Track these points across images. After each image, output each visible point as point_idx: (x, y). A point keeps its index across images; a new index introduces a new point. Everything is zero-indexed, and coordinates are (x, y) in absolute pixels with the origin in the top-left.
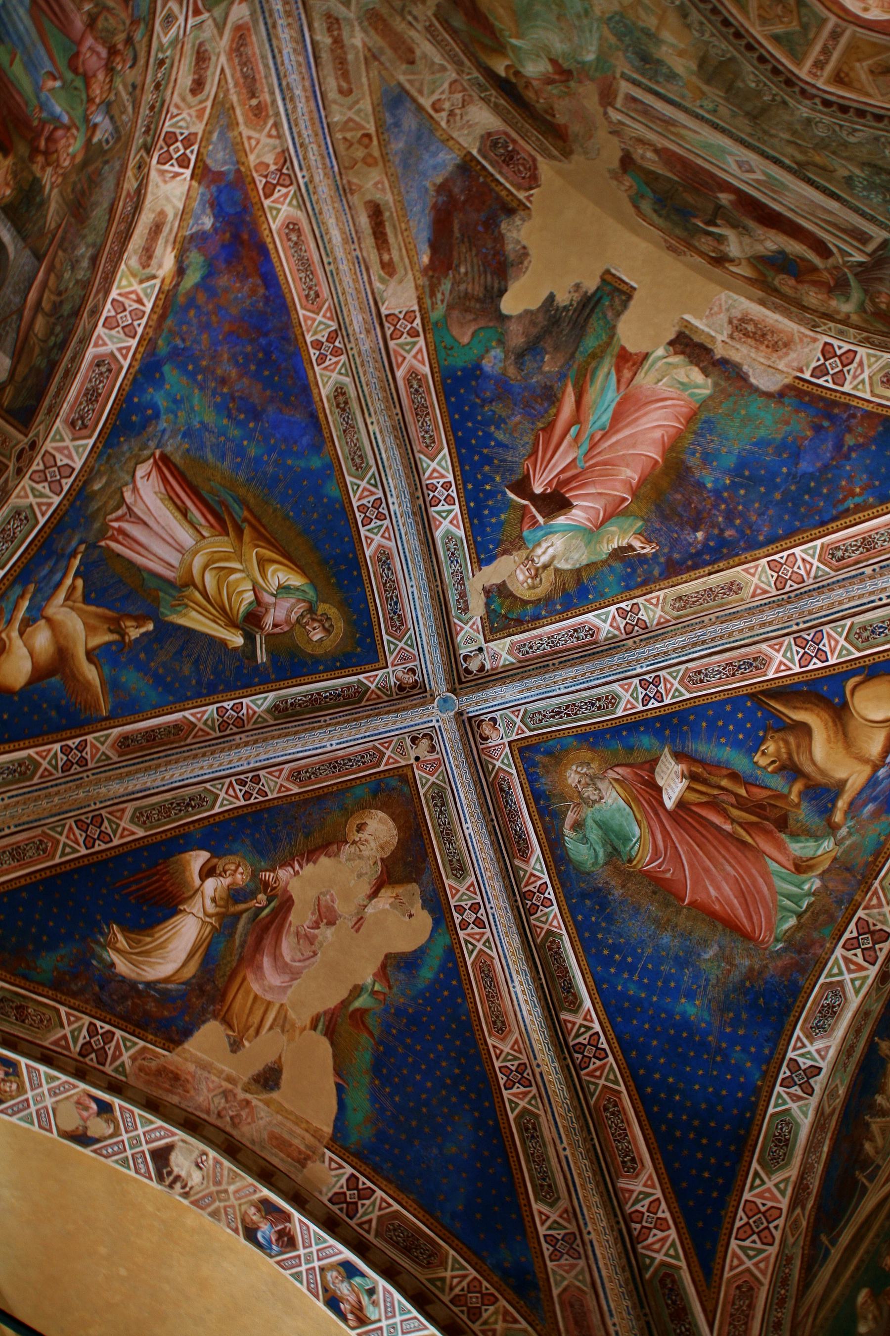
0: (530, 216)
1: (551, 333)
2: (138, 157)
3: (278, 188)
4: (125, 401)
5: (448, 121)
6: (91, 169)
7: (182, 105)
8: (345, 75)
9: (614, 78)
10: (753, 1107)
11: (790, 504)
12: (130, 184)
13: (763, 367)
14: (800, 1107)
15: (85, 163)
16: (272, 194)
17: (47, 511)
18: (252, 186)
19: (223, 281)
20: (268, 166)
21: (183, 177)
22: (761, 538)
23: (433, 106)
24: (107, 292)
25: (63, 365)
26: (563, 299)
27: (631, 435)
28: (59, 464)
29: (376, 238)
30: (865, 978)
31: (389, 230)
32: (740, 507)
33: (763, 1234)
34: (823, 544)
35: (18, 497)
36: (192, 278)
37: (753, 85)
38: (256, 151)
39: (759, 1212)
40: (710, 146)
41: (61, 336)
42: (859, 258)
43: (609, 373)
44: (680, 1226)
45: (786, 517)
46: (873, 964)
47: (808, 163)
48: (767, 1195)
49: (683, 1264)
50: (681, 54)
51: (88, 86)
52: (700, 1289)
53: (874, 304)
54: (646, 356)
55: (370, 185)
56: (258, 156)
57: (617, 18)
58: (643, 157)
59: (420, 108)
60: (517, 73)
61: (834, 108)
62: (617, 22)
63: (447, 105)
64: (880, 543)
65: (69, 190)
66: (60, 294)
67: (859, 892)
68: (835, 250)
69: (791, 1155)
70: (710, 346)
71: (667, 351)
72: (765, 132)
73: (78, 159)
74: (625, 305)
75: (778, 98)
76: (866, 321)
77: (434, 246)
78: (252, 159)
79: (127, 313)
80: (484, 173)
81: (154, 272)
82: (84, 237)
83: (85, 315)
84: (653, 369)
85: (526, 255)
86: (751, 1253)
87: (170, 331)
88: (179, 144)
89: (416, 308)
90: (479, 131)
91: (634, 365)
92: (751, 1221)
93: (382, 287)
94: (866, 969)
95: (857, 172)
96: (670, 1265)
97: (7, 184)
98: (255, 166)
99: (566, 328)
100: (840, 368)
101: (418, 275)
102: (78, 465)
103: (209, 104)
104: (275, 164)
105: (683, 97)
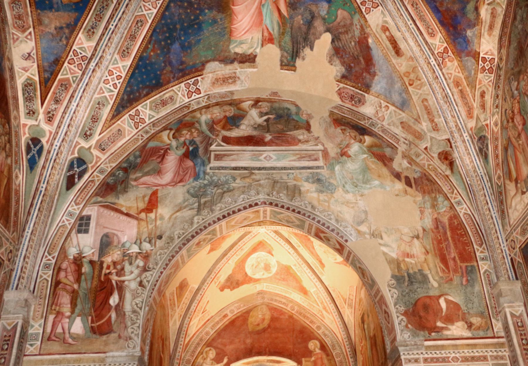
0: (335, 78)
1: (305, 34)
3: (442, 51)
5: (381, 103)
7: (488, 86)
8: (426, 108)
9: (326, 164)
11: (171, 27)
12: (504, 51)
13: (216, 70)
15: (520, 72)
16: (444, 48)
19: (456, 7)
20: (449, 61)
21: (484, 53)
22: (172, 5)
23: (388, 107)
26: (307, 50)
27: (250, 10)
29: (395, 40)
31: (390, 46)
32: (189, 11)
34: (148, 22)
36: (470, 7)
37: (281, 195)
38: (455, 67)
40: (283, 158)
42: (213, 147)
43: (273, 30)
45: (169, 21)
47: (250, 176)
50: (308, 191)
51: (520, 108)
53: (197, 129)
54: (262, 46)
55: (404, 64)
56: (454, 64)
57: (333, 191)
58: (303, 134)
59: (393, 105)
60: (360, 141)
61: (253, 204)
62: (333, 189)
63: (383, 109)
64: (129, 42)
68: (223, 144)
70: (241, 64)
71: (256, 52)
72: (269, 179)
73: (521, 77)
74: (282, 61)
75: (271, 195)
76: (194, 117)
77: (368, 48)
78: (456, 63)
80: (359, 88)
81: (489, 7)
82: (519, 33)
84: (256, 42)
85: (330, 62)
88: (487, 68)
89: (367, 16)
90: (367, 104)
91: (265, 40)
93: (385, 19)
95: (234, 185)
99: (300, 39)
100: (190, 89)
101: (371, 32)
103: (477, 87)
104: (446, 62)
105: (300, 173)
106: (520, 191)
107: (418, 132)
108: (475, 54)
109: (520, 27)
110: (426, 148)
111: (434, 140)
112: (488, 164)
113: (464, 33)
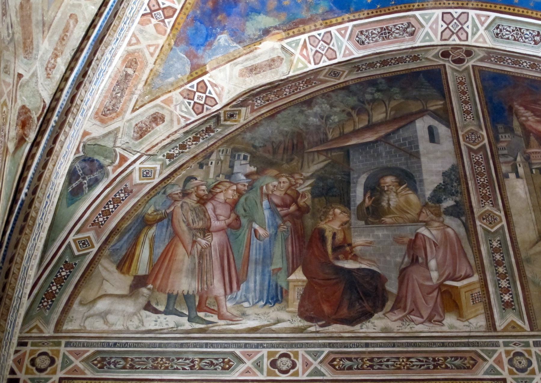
2: (228, 123)
3: (162, 6)
4: (375, 7)
6: (270, 157)
7: (175, 119)
8: (66, 30)
15: (271, 164)
17: (483, 16)
18: (176, 26)
20: (155, 26)
21: (211, 80)
24: (316, 72)
25: (382, 72)
28: (445, 26)
35: (485, 42)
38: (154, 42)
41: (369, 90)
56: (156, 38)
65: (294, 163)
66: (349, 114)
78: (161, 41)
79: (318, 49)
81: (280, 51)
83: (342, 80)
87: (308, 10)
88: (196, 100)
97: (334, 214)
98: (164, 35)
102: (439, 12)
103: (158, 101)
104: (150, 21)
106: (142, 301)
107: (32, 42)
108: (199, 66)
109: (314, 120)
110: (20, 76)
111: (34, 80)
112: (69, 205)
113: (219, 30)
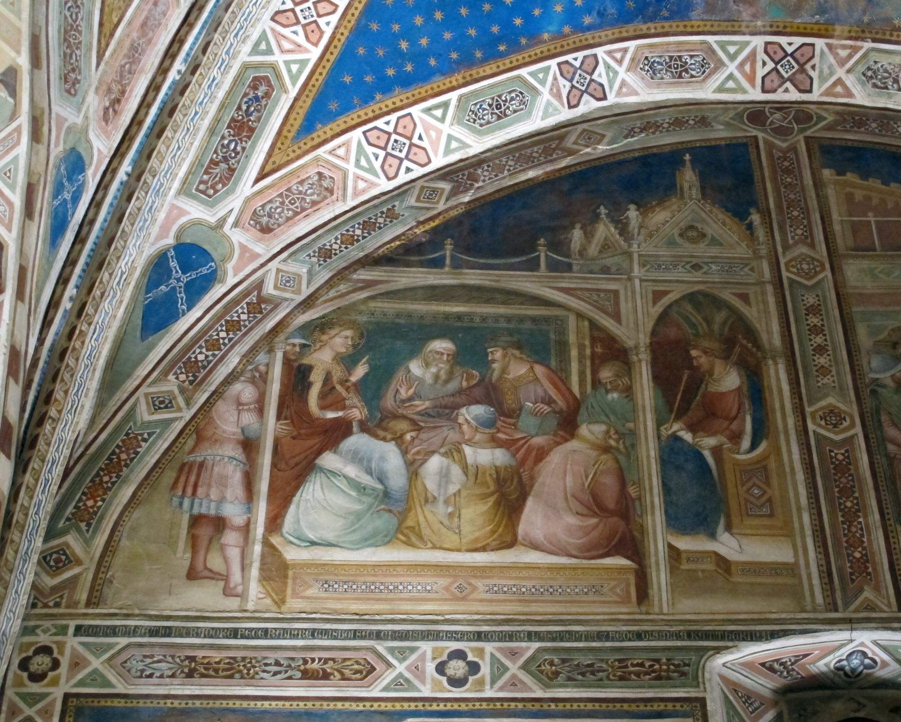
10: (515, 47)
14: (549, 104)
30: (741, 90)
33: (390, 160)
39: (410, 139)
44: (328, 56)
46: (764, 91)
48: (433, 134)
49: (293, 92)
52: (285, 133)
67: (846, 28)
69: (492, 131)
86: (363, 162)
92: (394, 137)
94: (753, 86)
96: (279, 76)
